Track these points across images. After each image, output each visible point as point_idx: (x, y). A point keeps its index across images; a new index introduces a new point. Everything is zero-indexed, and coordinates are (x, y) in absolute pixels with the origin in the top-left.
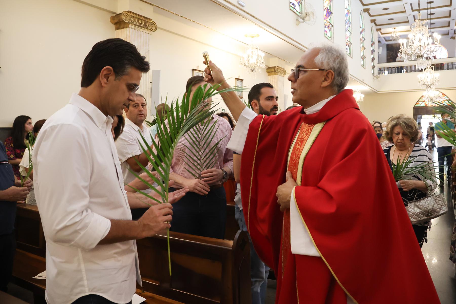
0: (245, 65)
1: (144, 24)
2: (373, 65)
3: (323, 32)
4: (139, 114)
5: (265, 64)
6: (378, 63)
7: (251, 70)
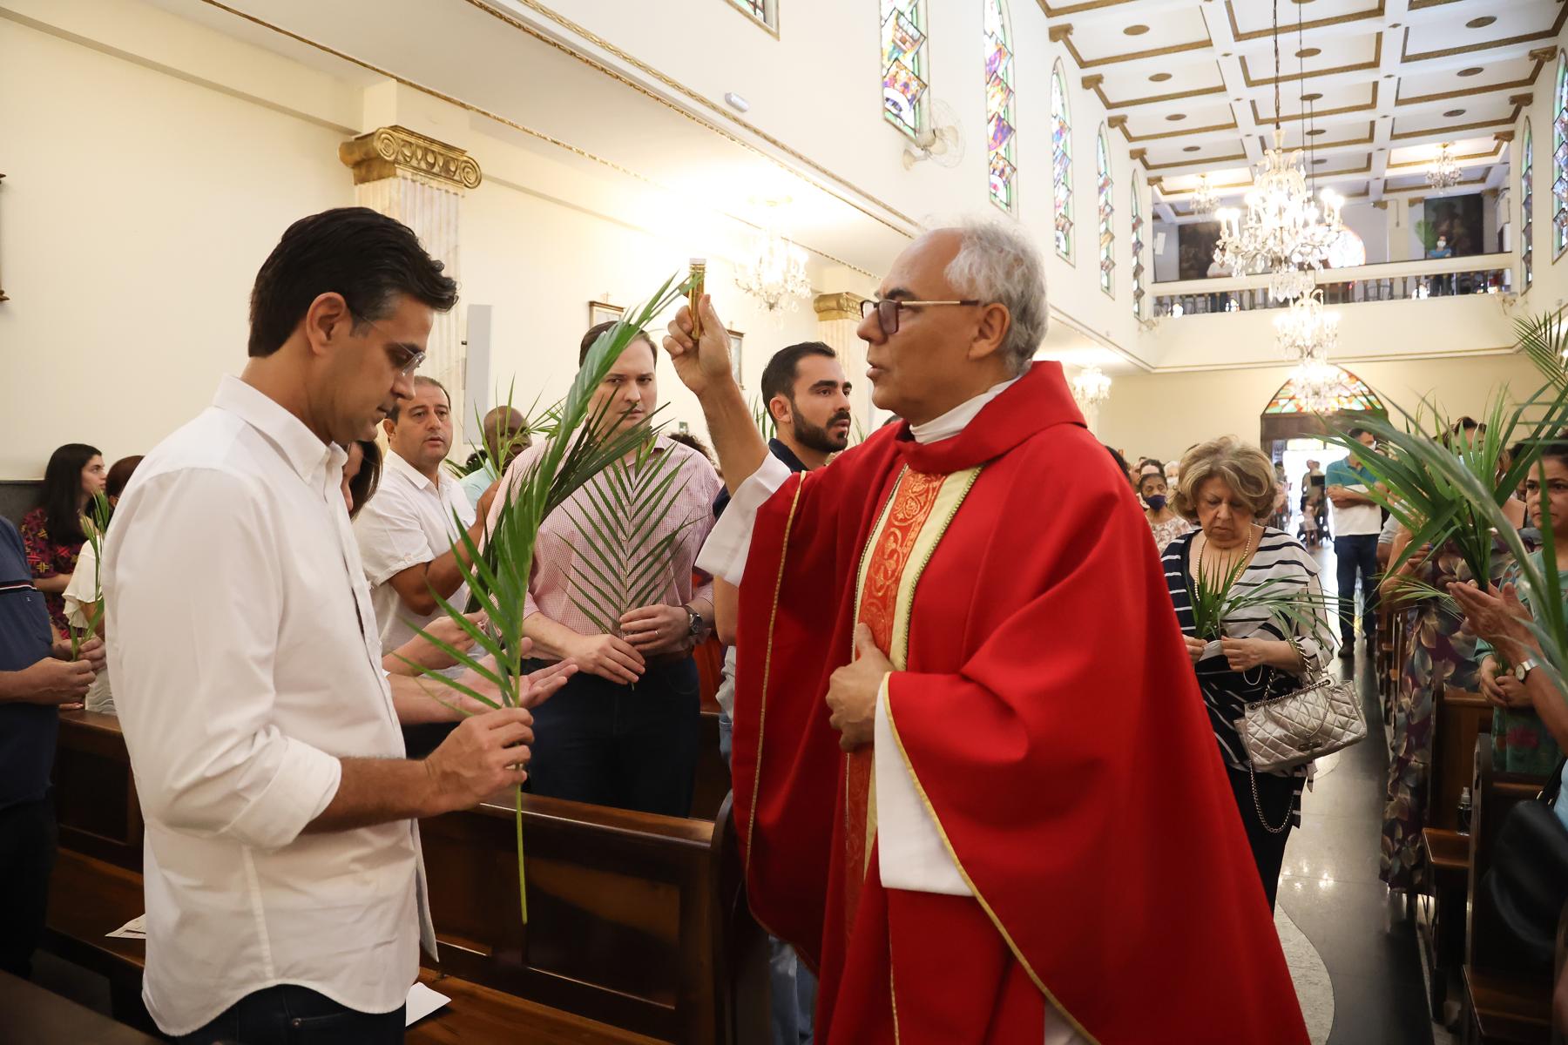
0: (749, 290)
1: (441, 165)
2: (1138, 288)
3: (987, 189)
4: (429, 437)
5: (809, 286)
6: (1152, 280)
7: (766, 304)
